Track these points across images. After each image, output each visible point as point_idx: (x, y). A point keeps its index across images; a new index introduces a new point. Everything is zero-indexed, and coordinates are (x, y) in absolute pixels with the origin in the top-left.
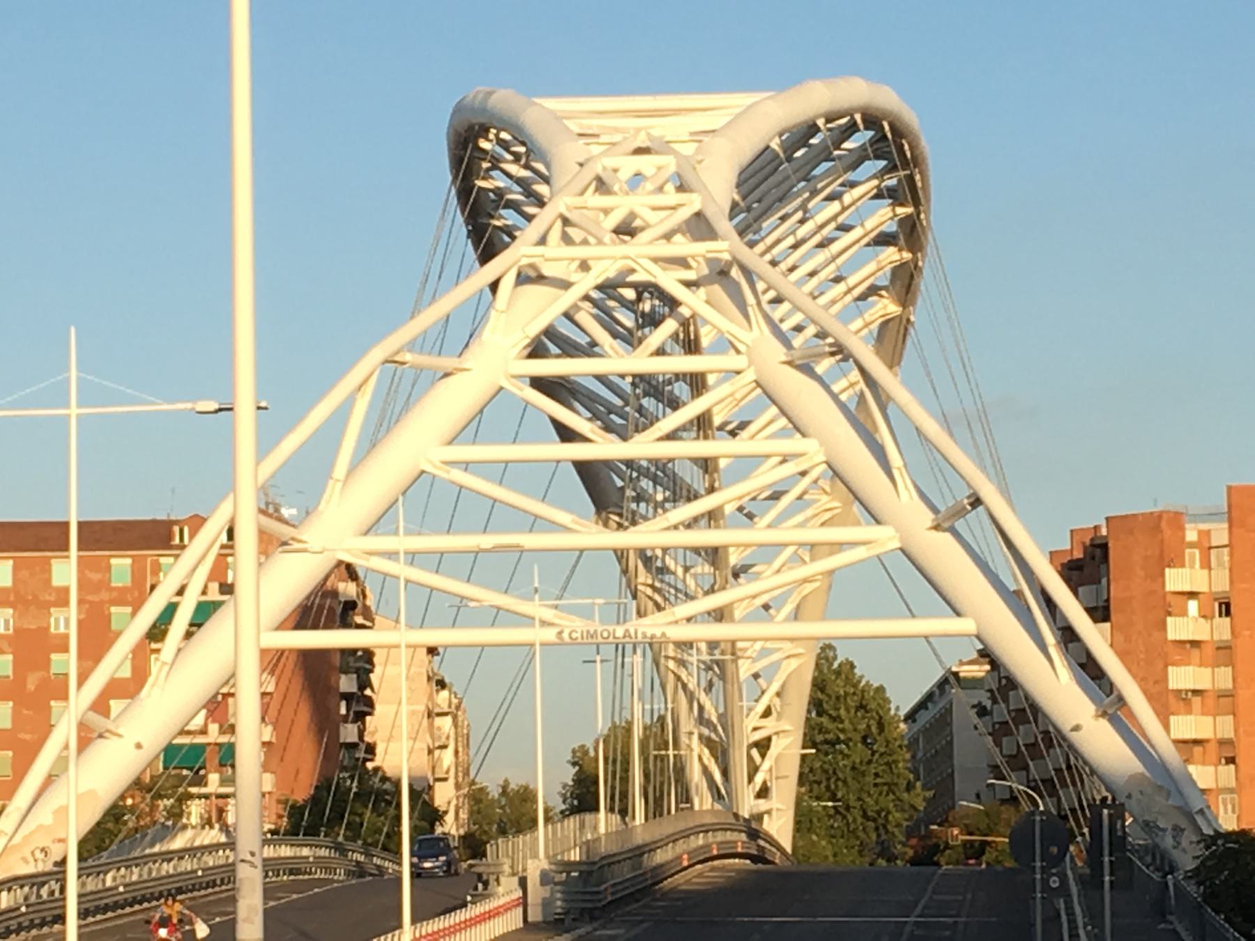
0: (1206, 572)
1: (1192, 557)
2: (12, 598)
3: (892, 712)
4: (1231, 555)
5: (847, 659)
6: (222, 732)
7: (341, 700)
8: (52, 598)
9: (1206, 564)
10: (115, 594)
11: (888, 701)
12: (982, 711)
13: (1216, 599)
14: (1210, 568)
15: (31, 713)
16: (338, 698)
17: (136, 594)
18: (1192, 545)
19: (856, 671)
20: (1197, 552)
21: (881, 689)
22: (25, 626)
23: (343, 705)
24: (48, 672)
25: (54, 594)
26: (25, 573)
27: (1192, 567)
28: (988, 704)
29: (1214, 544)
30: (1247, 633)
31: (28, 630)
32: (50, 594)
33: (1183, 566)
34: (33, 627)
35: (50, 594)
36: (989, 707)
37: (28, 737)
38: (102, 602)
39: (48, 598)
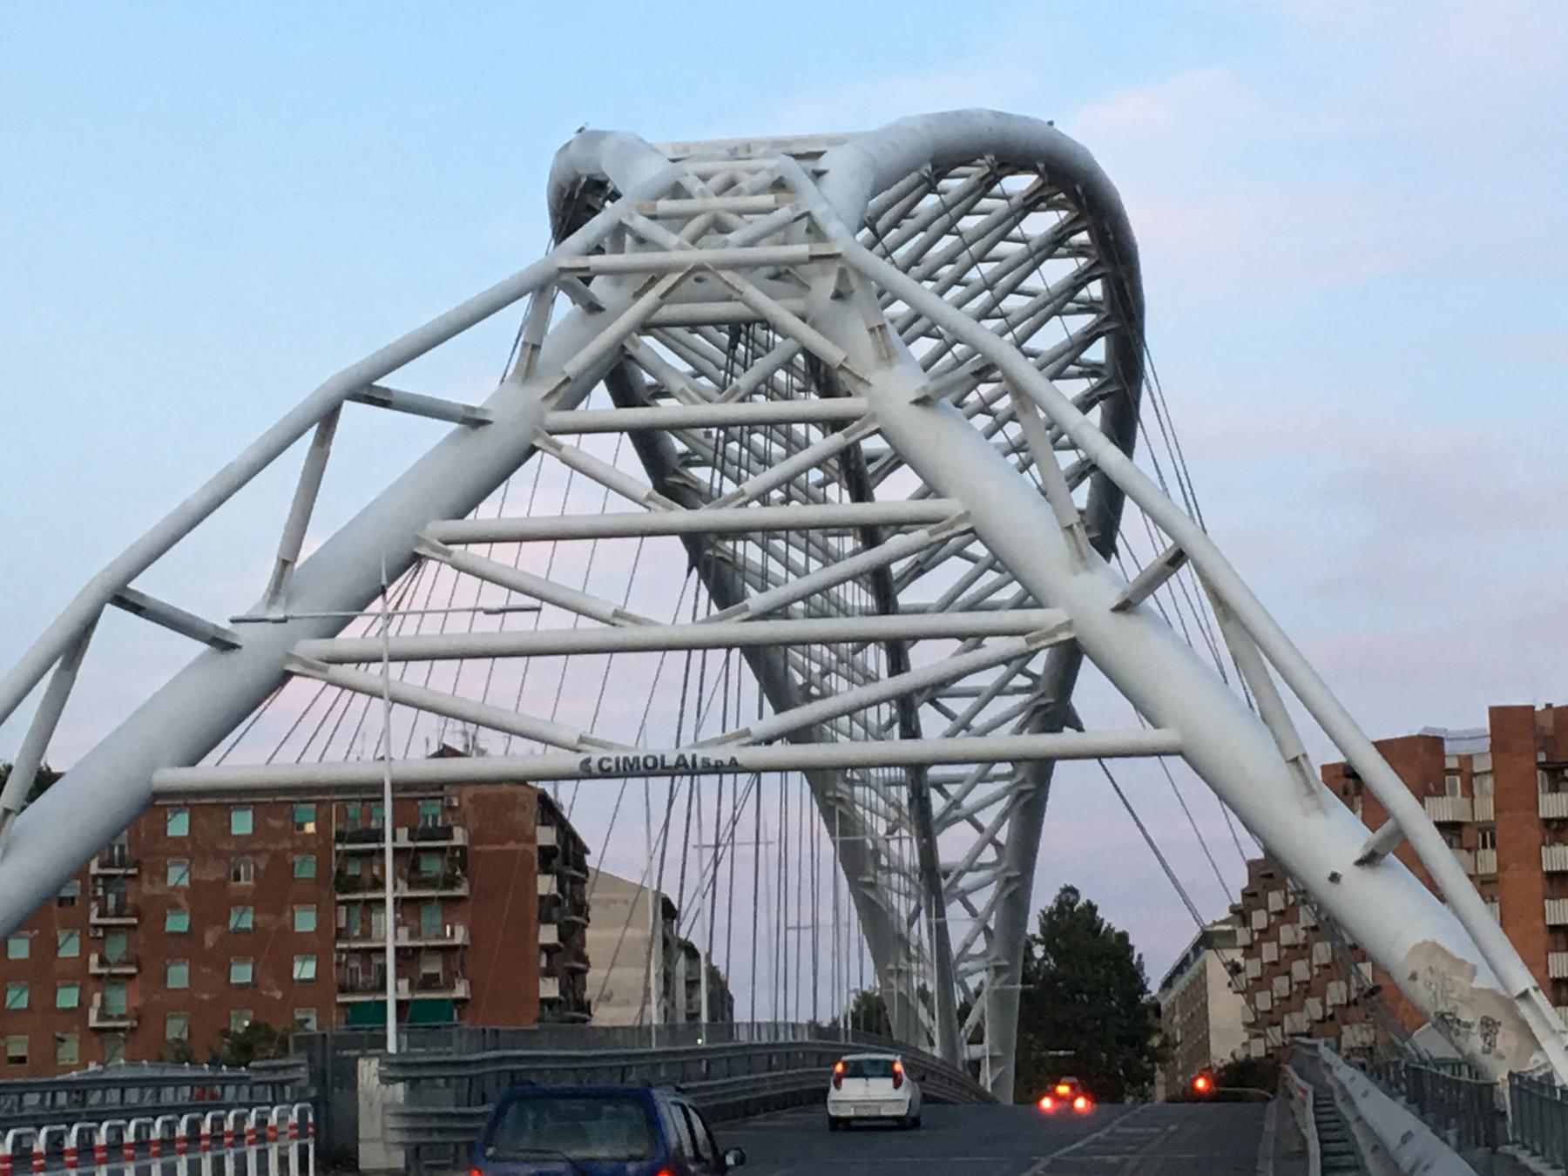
0: (1466, 801)
1: (1453, 787)
2: (189, 848)
3: (1134, 962)
4: (1496, 781)
5: (1089, 902)
6: (411, 987)
7: (540, 953)
8: (232, 847)
9: (1468, 791)
10: (298, 842)
11: (1131, 948)
12: (1235, 969)
13: (1479, 830)
14: (1473, 797)
15: (209, 970)
16: (538, 949)
17: (321, 842)
18: (1451, 772)
19: (1099, 914)
20: (1458, 779)
21: (1123, 937)
22: (204, 878)
23: (544, 957)
24: (228, 926)
25: (233, 844)
26: (203, 821)
27: (1453, 794)
28: (1240, 960)
29: (1476, 770)
30: (1514, 865)
31: (208, 881)
32: (229, 844)
33: (1443, 794)
34: (212, 879)
35: (229, 844)
36: (1242, 964)
37: (205, 997)
38: (286, 850)
39: (225, 847)
